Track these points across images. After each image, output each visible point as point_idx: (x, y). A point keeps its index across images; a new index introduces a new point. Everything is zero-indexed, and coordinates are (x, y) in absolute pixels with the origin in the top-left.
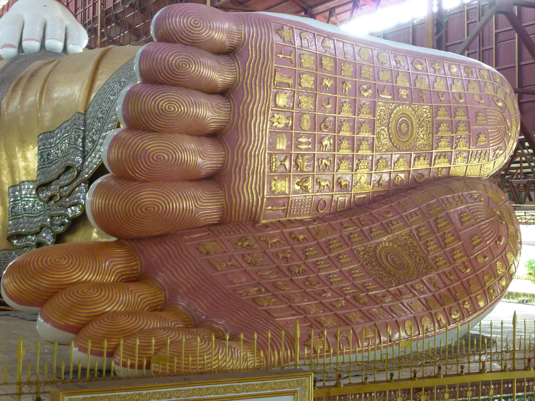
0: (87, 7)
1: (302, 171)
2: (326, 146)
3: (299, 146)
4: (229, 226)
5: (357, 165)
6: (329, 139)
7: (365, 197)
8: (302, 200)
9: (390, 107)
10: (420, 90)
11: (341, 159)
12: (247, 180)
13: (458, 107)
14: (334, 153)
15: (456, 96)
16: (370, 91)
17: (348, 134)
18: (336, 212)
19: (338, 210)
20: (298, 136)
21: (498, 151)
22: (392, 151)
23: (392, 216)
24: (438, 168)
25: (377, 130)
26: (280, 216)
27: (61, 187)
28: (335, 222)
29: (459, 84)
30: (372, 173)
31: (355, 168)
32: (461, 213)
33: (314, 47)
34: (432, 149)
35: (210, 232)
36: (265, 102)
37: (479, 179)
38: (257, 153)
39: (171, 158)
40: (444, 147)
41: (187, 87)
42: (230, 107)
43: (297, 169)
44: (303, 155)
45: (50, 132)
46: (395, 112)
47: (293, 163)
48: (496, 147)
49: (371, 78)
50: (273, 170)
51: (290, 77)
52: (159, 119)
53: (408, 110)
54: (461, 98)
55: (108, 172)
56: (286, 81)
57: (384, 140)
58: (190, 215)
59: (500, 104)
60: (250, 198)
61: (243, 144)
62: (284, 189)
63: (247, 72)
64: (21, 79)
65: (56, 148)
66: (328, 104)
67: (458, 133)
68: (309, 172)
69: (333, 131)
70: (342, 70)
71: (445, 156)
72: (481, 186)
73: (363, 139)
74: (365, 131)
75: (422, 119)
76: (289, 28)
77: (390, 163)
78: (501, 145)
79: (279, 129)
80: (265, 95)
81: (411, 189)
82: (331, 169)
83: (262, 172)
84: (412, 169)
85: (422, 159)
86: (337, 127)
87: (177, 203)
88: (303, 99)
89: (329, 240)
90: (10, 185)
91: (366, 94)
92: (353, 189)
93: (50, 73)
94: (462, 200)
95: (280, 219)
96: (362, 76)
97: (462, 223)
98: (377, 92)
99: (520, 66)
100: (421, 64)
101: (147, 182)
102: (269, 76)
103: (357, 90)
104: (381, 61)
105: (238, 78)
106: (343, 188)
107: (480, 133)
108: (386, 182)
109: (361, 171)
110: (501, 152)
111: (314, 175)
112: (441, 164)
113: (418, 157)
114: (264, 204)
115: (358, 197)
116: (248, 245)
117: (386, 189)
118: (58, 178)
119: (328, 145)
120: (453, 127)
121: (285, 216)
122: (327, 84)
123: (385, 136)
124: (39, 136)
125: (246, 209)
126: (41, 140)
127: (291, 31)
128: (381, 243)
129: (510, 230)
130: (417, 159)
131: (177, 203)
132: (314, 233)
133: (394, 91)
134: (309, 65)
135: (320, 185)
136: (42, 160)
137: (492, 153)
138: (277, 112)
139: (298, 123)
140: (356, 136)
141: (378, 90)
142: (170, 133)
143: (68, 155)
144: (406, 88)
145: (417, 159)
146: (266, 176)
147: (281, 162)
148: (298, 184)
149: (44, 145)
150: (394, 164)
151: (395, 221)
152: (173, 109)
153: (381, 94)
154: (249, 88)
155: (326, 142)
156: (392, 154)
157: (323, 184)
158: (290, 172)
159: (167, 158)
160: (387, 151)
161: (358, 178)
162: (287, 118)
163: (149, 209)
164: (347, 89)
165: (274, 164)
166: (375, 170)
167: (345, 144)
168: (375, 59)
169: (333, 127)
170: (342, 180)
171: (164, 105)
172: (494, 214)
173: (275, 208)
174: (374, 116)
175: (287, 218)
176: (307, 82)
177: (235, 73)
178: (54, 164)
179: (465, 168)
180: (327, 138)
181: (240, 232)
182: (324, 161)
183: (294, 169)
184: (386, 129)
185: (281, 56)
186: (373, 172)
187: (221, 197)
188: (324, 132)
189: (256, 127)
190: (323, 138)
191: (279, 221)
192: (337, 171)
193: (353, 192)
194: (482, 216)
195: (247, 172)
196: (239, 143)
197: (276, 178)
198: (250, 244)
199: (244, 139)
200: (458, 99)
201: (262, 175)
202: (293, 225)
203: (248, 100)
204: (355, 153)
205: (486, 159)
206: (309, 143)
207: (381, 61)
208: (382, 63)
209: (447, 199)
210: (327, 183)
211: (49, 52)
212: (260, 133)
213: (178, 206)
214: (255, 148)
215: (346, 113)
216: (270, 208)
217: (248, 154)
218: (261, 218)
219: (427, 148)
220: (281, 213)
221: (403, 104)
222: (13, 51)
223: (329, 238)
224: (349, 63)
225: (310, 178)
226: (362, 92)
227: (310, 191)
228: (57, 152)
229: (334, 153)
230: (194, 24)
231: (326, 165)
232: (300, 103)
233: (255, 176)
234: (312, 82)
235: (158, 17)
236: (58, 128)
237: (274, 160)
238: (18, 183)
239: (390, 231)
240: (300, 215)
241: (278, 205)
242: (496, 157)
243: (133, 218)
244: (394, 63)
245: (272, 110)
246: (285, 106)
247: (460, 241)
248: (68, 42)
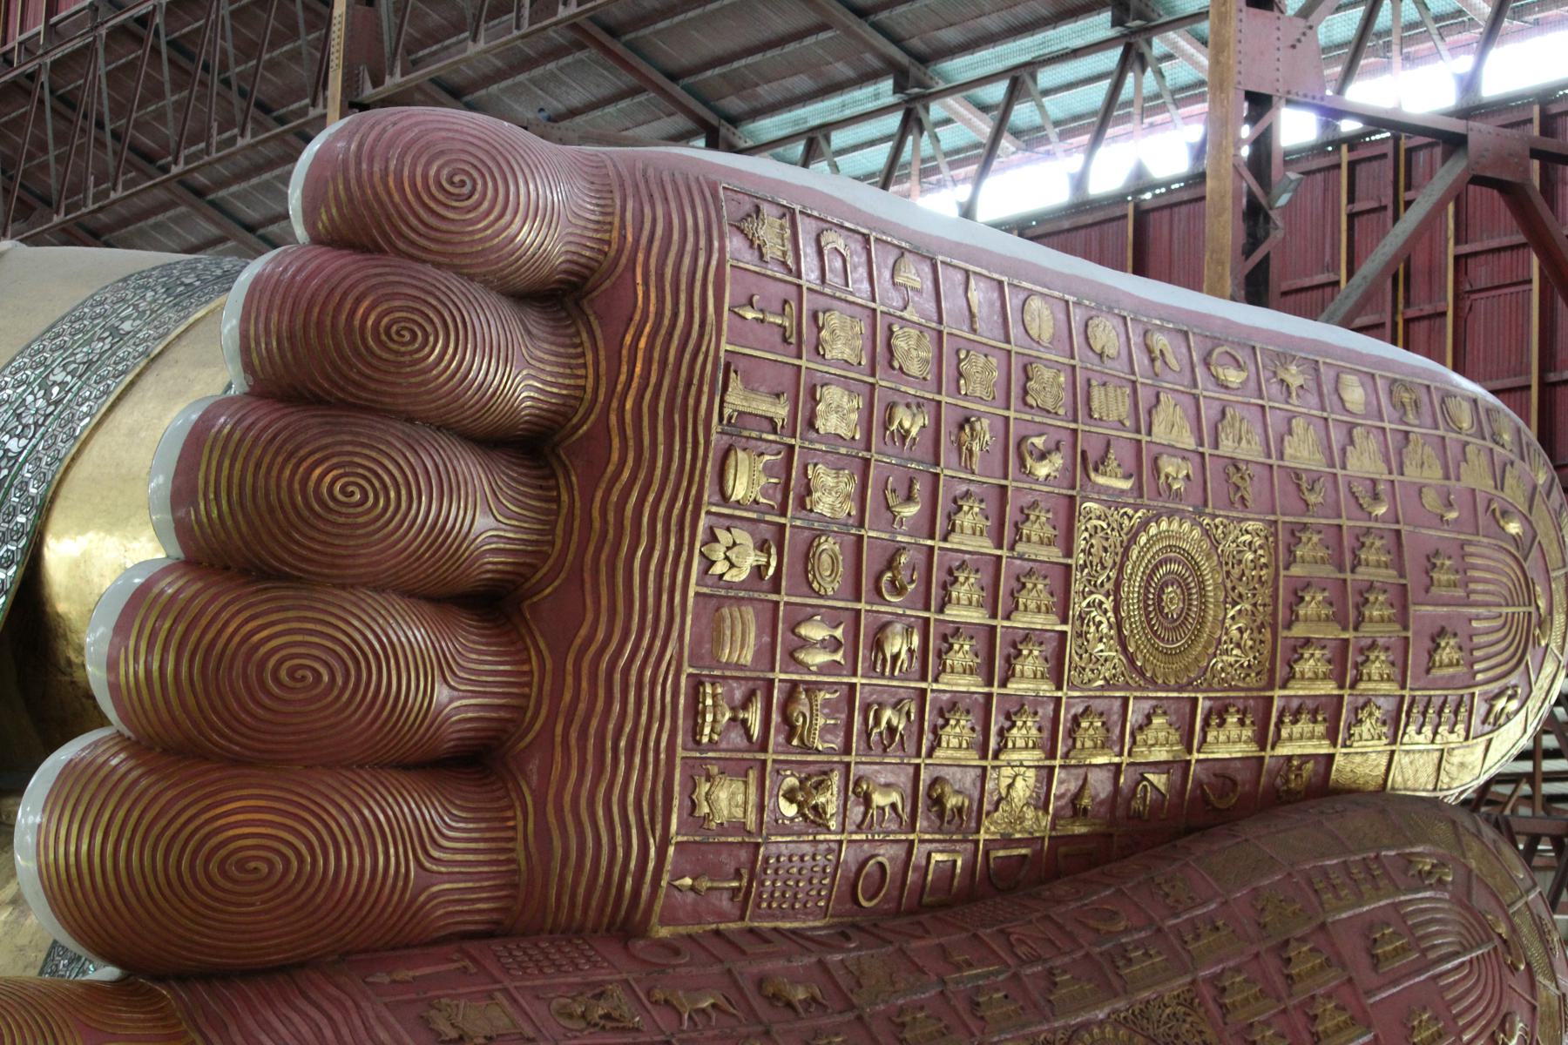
1: (806, 748)
2: (895, 657)
3: (801, 656)
4: (536, 945)
5: (1002, 733)
6: (908, 632)
7: (1025, 856)
8: (802, 858)
9: (1126, 521)
10: (1235, 463)
11: (946, 711)
12: (608, 774)
13: (1368, 531)
14: (923, 685)
15: (1358, 489)
16: (1058, 460)
17: (977, 616)
18: (918, 908)
19: (926, 899)
20: (801, 616)
21: (1500, 704)
22: (1127, 687)
23: (1127, 931)
24: (1289, 758)
25: (1079, 605)
26: (723, 916)
28: (923, 943)
29: (1373, 444)
30: (1052, 768)
31: (993, 743)
32: (1371, 927)
33: (865, 286)
34: (1271, 686)
35: (467, 962)
36: (685, 484)
37: (1434, 804)
38: (648, 673)
39: (340, 681)
40: (1312, 680)
41: (410, 420)
42: (558, 500)
43: (789, 740)
44: (812, 688)
46: (1143, 540)
47: (776, 717)
48: (1495, 687)
49: (1061, 412)
50: (705, 740)
51: (778, 396)
52: (306, 530)
53: (1187, 533)
54: (1376, 497)
55: (103, 721)
56: (764, 406)
57: (1101, 646)
58: (396, 897)
59: (1514, 528)
60: (619, 841)
61: (600, 635)
62: (739, 813)
63: (624, 369)
66: (909, 498)
67: (1367, 628)
68: (831, 751)
69: (920, 605)
70: (961, 375)
71: (1314, 713)
72: (1443, 828)
73: (1027, 636)
74: (1032, 605)
75: (1236, 572)
76: (781, 211)
77: (1117, 731)
78: (1513, 679)
79: (731, 585)
80: (689, 456)
81: (1189, 831)
82: (910, 747)
83: (663, 744)
84: (1196, 756)
85: (1232, 719)
86: (934, 588)
87: (355, 849)
88: (823, 477)
89: (901, 1011)
91: (1042, 470)
92: (986, 822)
94: (1373, 876)
95: (722, 926)
96: (1030, 400)
97: (1376, 962)
98: (1084, 463)
99: (1545, 386)
100: (1239, 366)
101: (250, 764)
102: (706, 389)
103: (1015, 452)
104: (1098, 349)
105: (589, 390)
106: (955, 822)
107: (1442, 632)
108: (1102, 803)
109: (1015, 756)
110: (1514, 705)
111: (848, 765)
112: (1301, 742)
113: (1219, 713)
114: (668, 866)
115: (1001, 853)
116: (607, 1016)
117: (1098, 829)
119: (903, 655)
120: (1348, 607)
121: (737, 913)
122: (907, 424)
123: (1104, 628)
125: (601, 880)
127: (786, 222)
128: (1086, 1026)
129: (1542, 995)
130: (1215, 721)
131: (355, 849)
132: (844, 982)
133: (1144, 465)
134: (847, 354)
135: (867, 800)
137: (1480, 708)
138: (727, 523)
139: (799, 568)
140: (1000, 623)
141: (1084, 453)
142: (343, 587)
144: (1183, 454)
145: (1215, 721)
146: (678, 761)
147: (733, 709)
148: (790, 796)
150: (1133, 735)
151: (1136, 948)
152: (358, 496)
153: (1096, 470)
154: (629, 432)
155: (896, 644)
156: (1125, 700)
157: (879, 799)
158: (764, 749)
159: (326, 678)
160: (1108, 685)
161: (1005, 782)
162: (762, 547)
163: (252, 865)
164: (976, 448)
165: (709, 718)
166: (1066, 756)
167: (962, 654)
168: (1077, 339)
169: (922, 588)
170: (947, 789)
171: (325, 478)
172: (1488, 932)
173: (705, 884)
174: (1069, 553)
175: (747, 923)
176: (838, 414)
177: (581, 372)
179: (1384, 761)
180: (898, 627)
181: (576, 966)
182: (888, 714)
183: (781, 739)
184: (1108, 604)
185: (750, 315)
186: (1057, 762)
187: (510, 834)
188: (889, 603)
189: (651, 577)
190: (884, 627)
191: (717, 933)
192: (930, 755)
193: (983, 836)
194: (1445, 942)
195: (609, 744)
196: (583, 632)
197: (714, 770)
198: (616, 1014)
199: (604, 618)
200: (1365, 501)
201: (663, 756)
202: (764, 948)
203: (626, 474)
204: (995, 690)
205: (1460, 728)
206: (835, 645)
207: (1098, 349)
208: (1101, 355)
209: (1324, 872)
210: (895, 797)
212: (665, 598)
213: (357, 862)
214: (642, 653)
215: (970, 535)
216: (688, 881)
217: (617, 676)
218: (655, 919)
220: (725, 904)
221: (1171, 514)
223: (901, 1002)
224: (988, 351)
225: (836, 779)
226: (1029, 462)
227: (833, 824)
229: (923, 685)
230: (452, 183)
231: (892, 730)
232: (809, 493)
233: (637, 760)
234: (854, 416)
235: (318, 157)
237: (709, 702)
239: (1116, 983)
240: (792, 914)
241: (715, 872)
242: (1495, 721)
243: (194, 898)
244: (1140, 359)
245: (708, 513)
246: (756, 502)
247: (1369, 1028)
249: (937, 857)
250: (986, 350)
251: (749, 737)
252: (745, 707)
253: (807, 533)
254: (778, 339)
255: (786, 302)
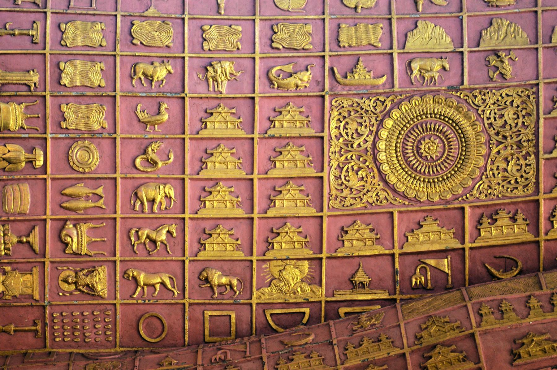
62: (29, 291)
75: (500, 122)
121: (43, 345)
175: (47, 350)
197: (8, 268)
219: (520, 192)
249: (210, 313)
250: (230, 22)
251: (34, 251)
252: (28, 236)
253: (67, 141)
254: (28, 43)
255: (34, 22)
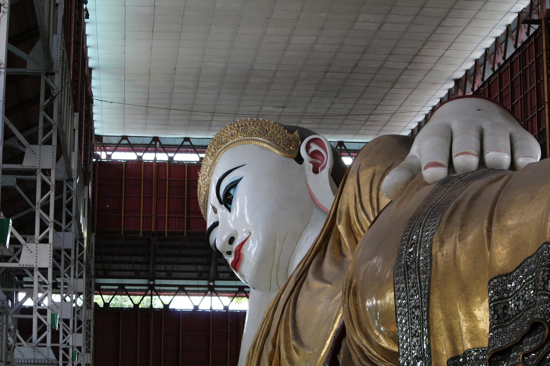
0: (529, 118)
27: (524, 355)
45: (506, 275)
64: (457, 205)
65: (516, 298)
90: (449, 357)
93: (500, 192)
118: (520, 342)
124: (489, 283)
126: (494, 287)
136: (496, 316)
143: (534, 306)
149: (496, 293)
178: (514, 321)
211: (492, 169)
222: (441, 172)
228: (517, 303)
236: (518, 268)
238: (461, 353)
248: (517, 154)
